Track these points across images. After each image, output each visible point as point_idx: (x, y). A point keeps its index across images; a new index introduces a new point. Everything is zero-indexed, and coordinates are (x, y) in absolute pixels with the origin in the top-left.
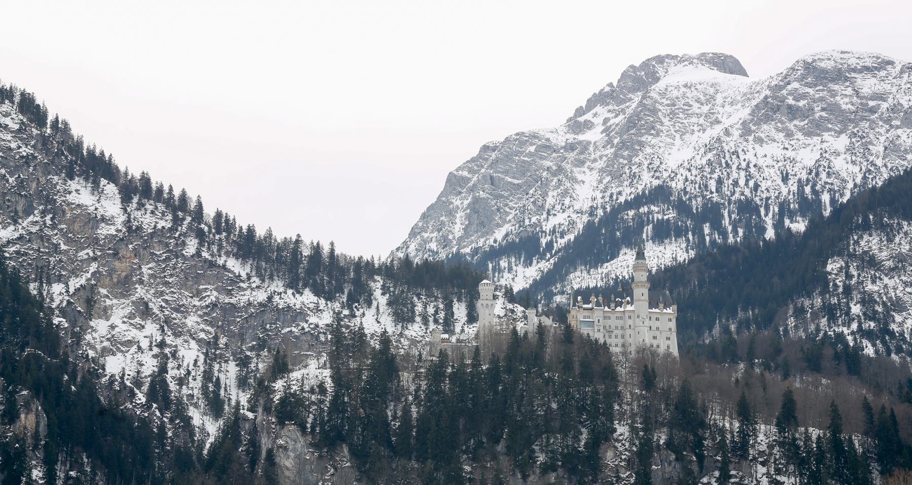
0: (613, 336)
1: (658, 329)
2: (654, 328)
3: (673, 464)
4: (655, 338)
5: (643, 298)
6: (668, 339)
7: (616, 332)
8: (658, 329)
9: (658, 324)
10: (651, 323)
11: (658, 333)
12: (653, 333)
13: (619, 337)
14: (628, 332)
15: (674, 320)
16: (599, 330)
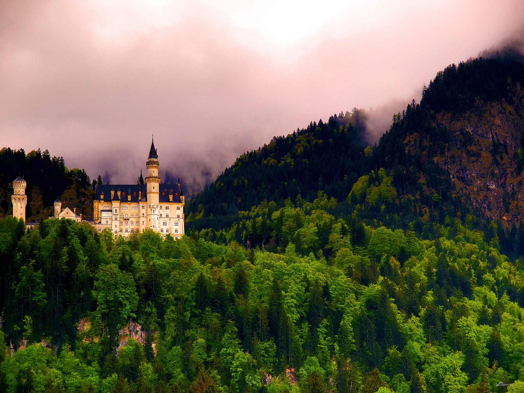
0: (129, 222)
1: (167, 216)
2: (164, 216)
3: (139, 333)
4: (165, 224)
5: (153, 191)
6: (176, 224)
7: (131, 219)
8: (167, 216)
9: (167, 212)
10: (161, 212)
11: (167, 220)
12: (162, 220)
13: (135, 223)
14: (142, 219)
15: (182, 209)
16: (116, 219)
